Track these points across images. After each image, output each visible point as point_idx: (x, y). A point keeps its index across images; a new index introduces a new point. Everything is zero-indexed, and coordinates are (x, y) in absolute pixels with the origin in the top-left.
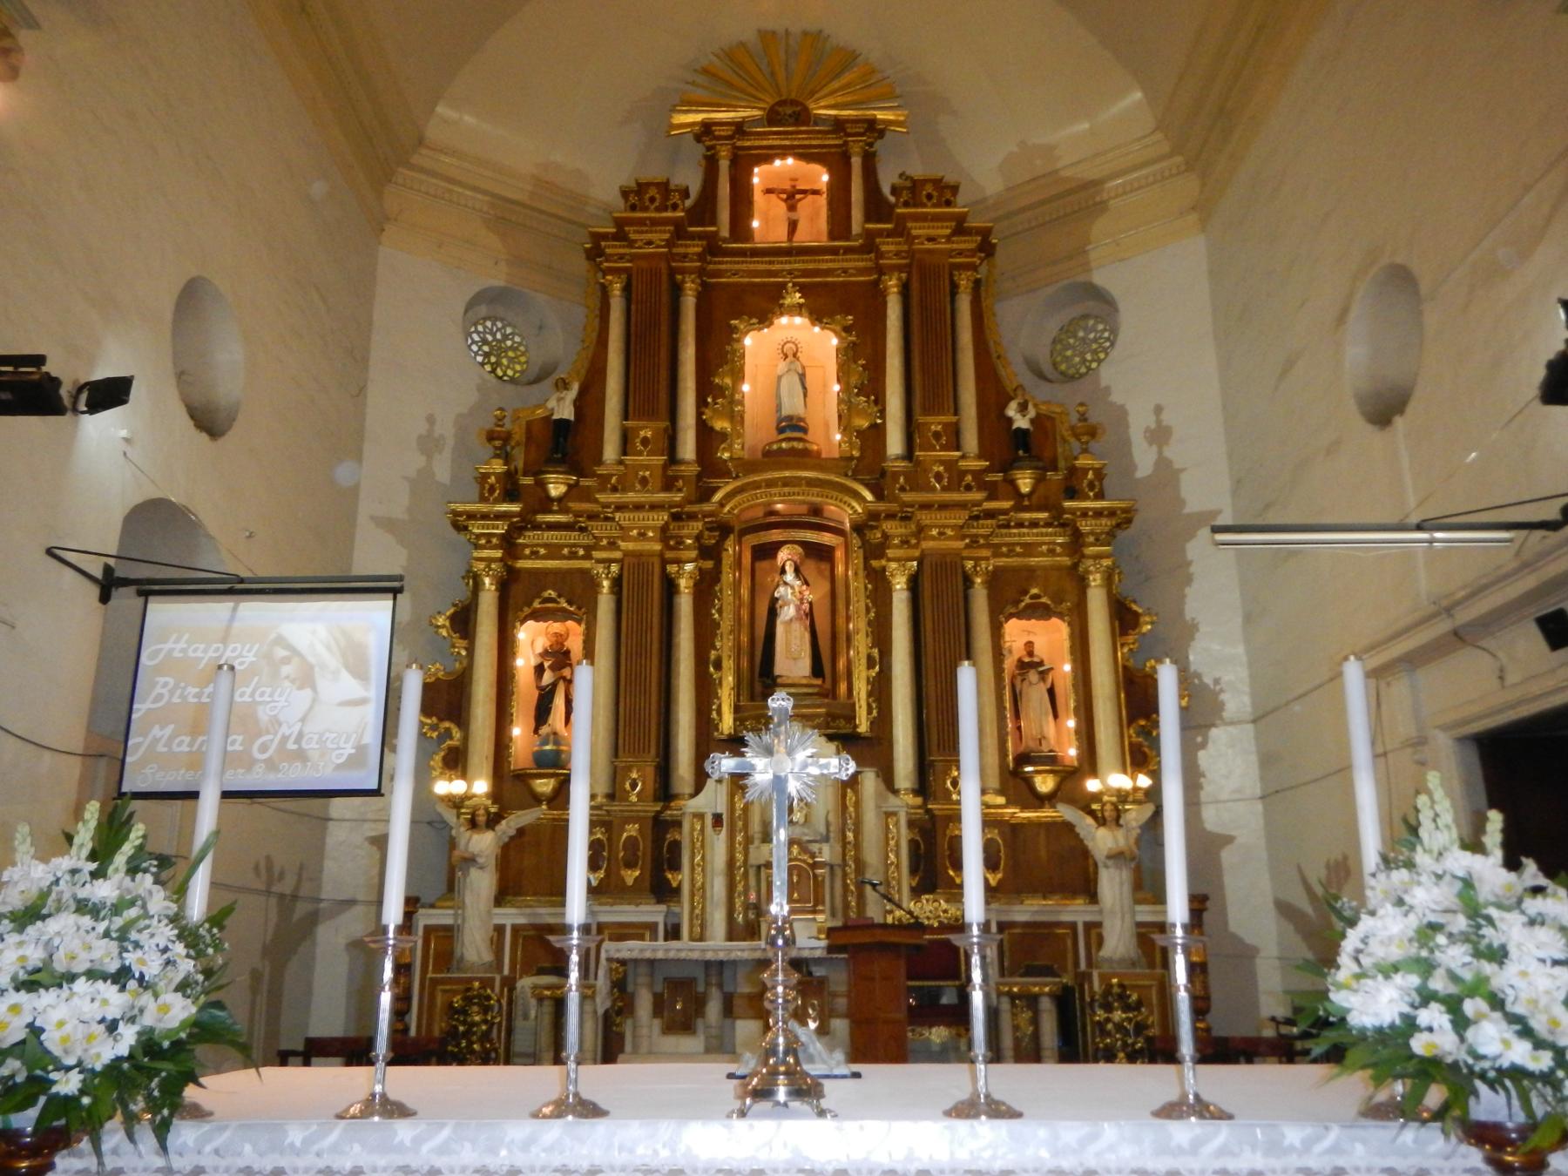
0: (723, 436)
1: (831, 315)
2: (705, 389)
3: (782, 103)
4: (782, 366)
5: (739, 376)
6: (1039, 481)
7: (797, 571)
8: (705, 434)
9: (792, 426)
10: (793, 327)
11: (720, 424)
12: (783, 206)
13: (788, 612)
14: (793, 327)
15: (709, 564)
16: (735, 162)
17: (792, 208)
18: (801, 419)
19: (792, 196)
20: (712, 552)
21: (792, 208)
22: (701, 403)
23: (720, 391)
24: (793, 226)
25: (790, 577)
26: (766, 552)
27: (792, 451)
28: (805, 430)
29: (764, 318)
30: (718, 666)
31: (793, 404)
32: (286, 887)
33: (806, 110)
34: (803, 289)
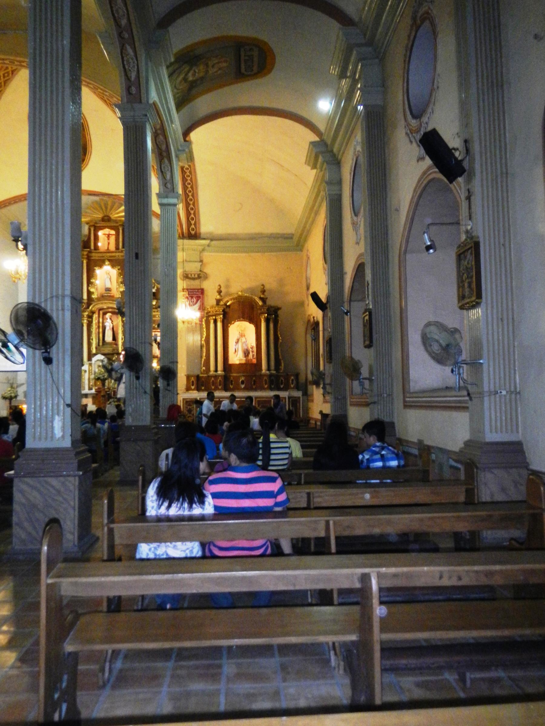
0: (93, 293)
1: (115, 266)
2: (89, 283)
3: (105, 216)
4: (106, 276)
5: (96, 279)
6: (156, 303)
7: (111, 319)
8: (89, 293)
9: (108, 290)
10: (107, 268)
11: (92, 290)
12: (106, 238)
13: (107, 328)
14: (107, 268)
15: (90, 320)
16: (94, 230)
17: (108, 239)
18: (110, 288)
19: (109, 236)
20: (90, 317)
21: (108, 239)
22: (88, 286)
23: (92, 283)
24: (109, 243)
25: (109, 320)
26: (104, 314)
27: (107, 296)
28: (110, 291)
29: (101, 266)
30: (92, 340)
31: (108, 285)
32: (11, 382)
33: (110, 218)
34: (109, 260)
